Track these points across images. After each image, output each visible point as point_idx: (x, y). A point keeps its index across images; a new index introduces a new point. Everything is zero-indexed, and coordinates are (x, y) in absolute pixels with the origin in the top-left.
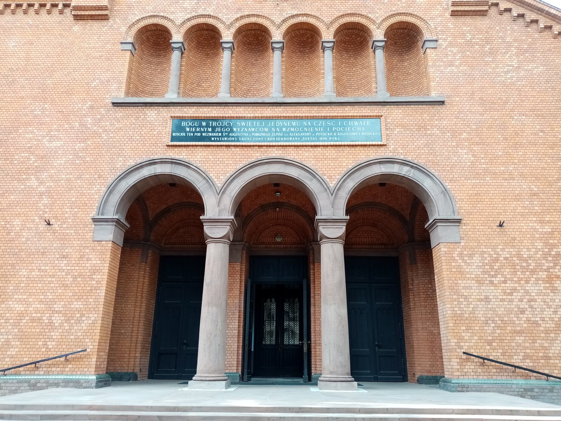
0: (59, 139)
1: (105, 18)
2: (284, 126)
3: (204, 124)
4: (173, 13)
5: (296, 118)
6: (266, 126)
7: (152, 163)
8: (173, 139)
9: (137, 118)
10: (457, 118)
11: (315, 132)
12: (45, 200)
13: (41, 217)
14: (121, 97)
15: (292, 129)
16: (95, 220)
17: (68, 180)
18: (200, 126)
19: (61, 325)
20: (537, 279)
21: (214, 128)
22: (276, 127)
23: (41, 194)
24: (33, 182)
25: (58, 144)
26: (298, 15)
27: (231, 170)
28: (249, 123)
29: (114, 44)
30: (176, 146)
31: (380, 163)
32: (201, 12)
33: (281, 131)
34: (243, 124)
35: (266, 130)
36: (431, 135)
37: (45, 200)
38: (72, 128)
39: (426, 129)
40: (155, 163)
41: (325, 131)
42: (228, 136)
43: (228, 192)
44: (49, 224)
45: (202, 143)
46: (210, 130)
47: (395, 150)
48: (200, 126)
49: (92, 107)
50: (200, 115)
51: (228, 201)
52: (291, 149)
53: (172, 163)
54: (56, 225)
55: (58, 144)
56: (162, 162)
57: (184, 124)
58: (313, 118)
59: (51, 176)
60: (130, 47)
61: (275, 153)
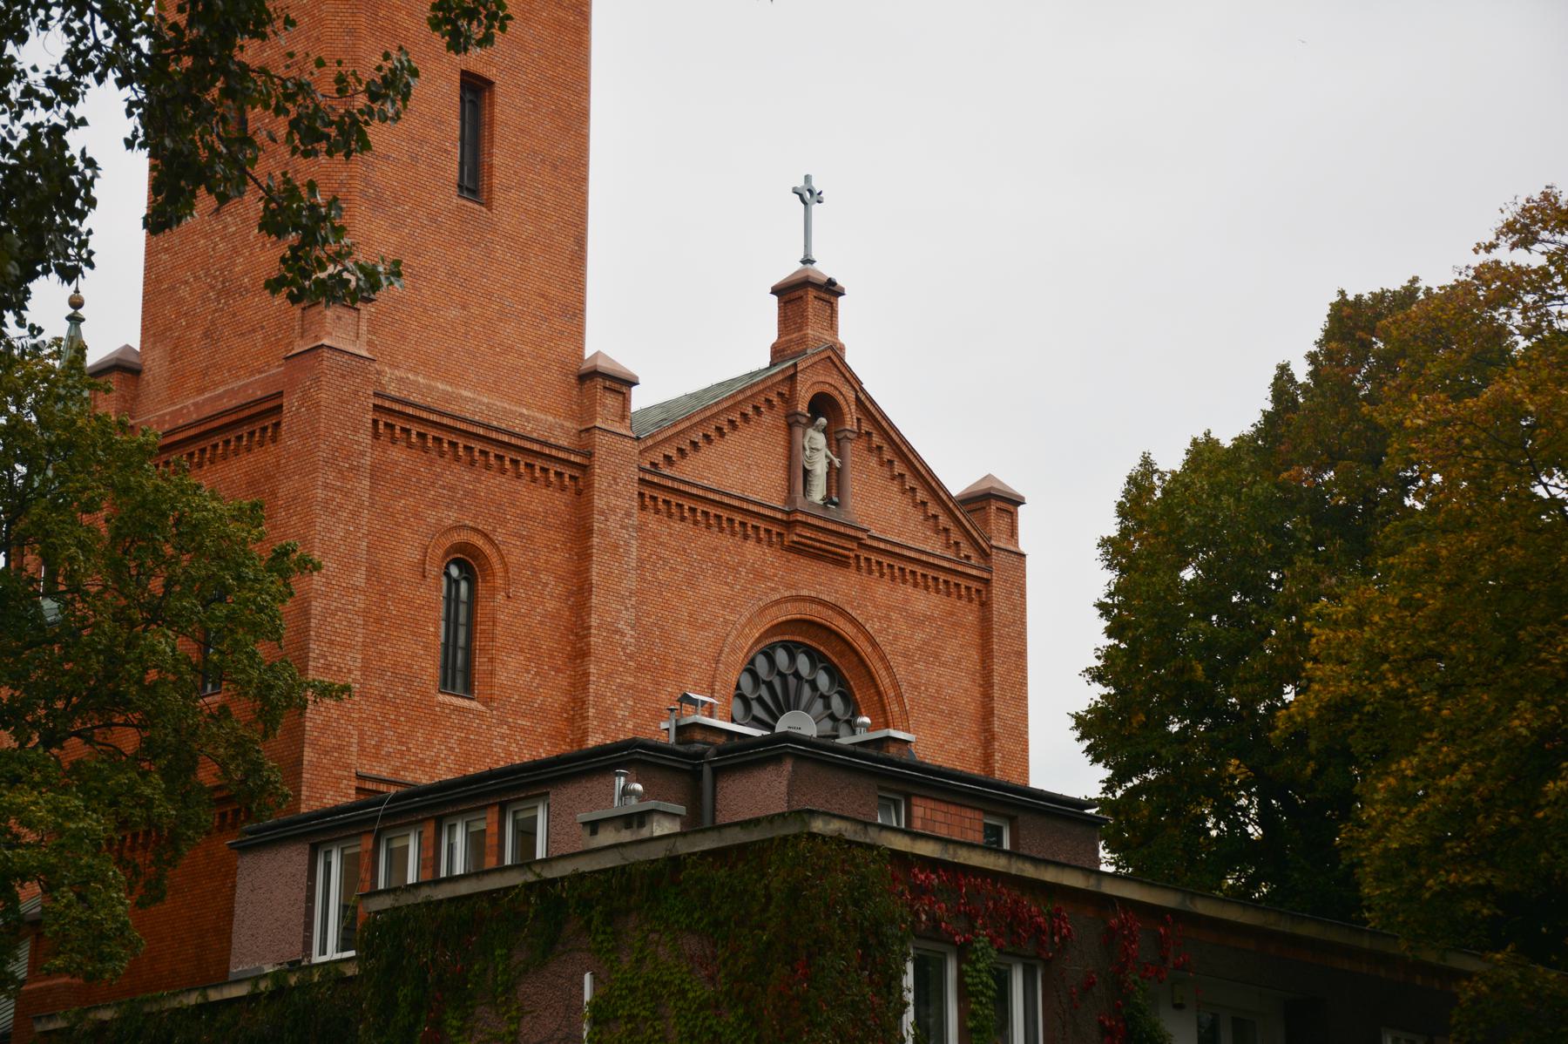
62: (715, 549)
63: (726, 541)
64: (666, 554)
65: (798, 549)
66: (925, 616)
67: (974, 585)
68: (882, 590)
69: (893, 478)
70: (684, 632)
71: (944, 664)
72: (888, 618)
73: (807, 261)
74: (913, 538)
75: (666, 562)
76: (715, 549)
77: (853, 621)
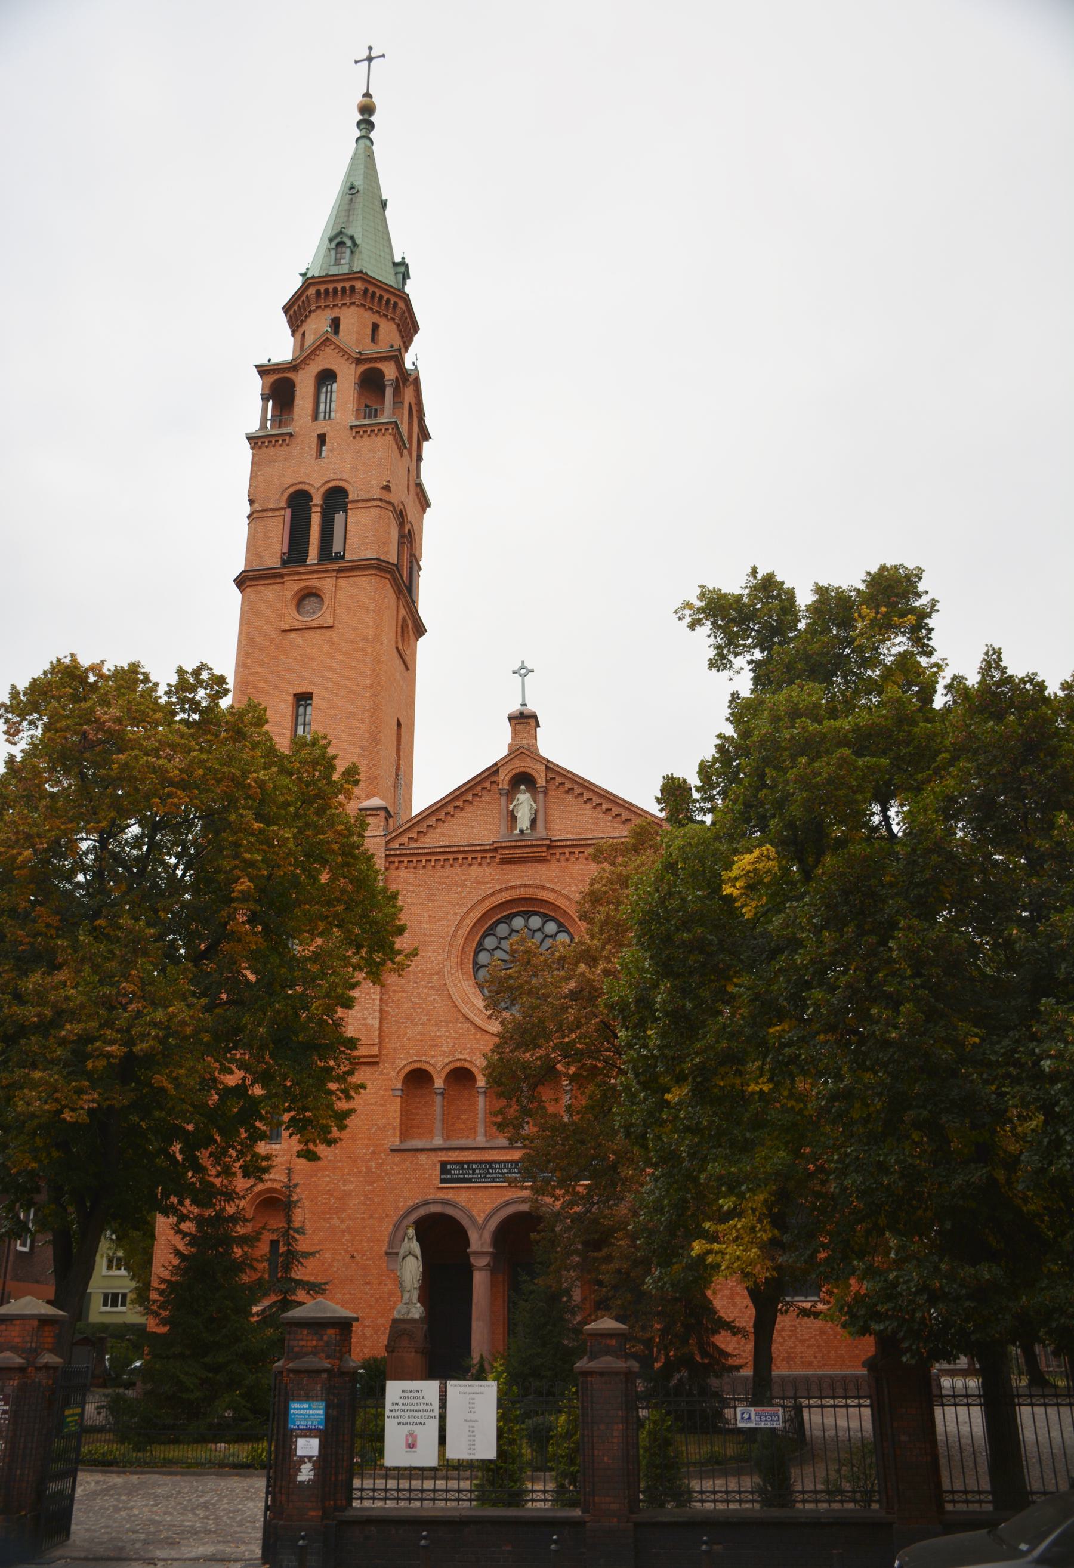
0: (352, 1183)
1: (377, 1063)
4: (433, 1057)
7: (426, 1203)
9: (411, 1162)
12: (347, 1237)
13: (346, 1251)
14: (396, 1142)
16: (387, 1254)
17: (363, 1218)
18: (463, 1168)
19: (371, 1336)
20: (723, 1296)
21: (474, 1170)
23: (343, 1231)
24: (335, 1221)
25: (352, 1186)
27: (489, 1208)
28: (502, 1166)
29: (386, 1090)
37: (347, 1237)
38: (360, 1172)
44: (353, 1256)
48: (463, 1168)
49: (374, 1152)
51: (487, 1235)
54: (358, 1258)
55: (352, 1186)
57: (449, 1167)
59: (349, 1216)
60: (399, 1093)
62: (448, 877)
63: (457, 870)
64: (410, 888)
65: (504, 861)
69: (585, 802)
70: (425, 926)
73: (524, 705)
74: (603, 832)
75: (412, 892)
76: (448, 877)
77: (552, 890)
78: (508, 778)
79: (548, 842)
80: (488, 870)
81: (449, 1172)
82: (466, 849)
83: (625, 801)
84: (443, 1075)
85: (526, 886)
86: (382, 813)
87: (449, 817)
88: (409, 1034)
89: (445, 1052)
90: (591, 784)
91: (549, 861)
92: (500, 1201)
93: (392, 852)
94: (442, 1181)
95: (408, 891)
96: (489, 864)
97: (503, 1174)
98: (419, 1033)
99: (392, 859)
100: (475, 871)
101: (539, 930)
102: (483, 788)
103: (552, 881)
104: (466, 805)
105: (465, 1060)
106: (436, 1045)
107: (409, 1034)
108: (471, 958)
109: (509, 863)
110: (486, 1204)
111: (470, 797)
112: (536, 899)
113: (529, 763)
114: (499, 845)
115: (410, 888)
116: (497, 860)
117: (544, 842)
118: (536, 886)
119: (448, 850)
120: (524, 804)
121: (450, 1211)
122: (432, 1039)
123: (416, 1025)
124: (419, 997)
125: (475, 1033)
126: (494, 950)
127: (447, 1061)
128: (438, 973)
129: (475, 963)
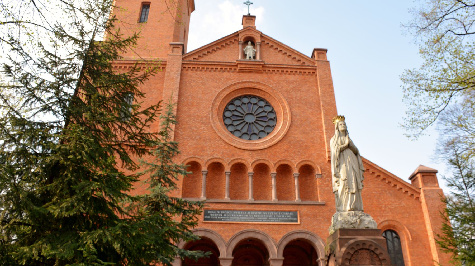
2: (255, 214)
3: (219, 212)
4: (202, 156)
5: (260, 211)
6: (246, 214)
8: (205, 219)
10: (330, 212)
11: (268, 217)
15: (259, 216)
18: (217, 213)
21: (223, 214)
22: (251, 215)
26: (260, 160)
27: (231, 235)
28: (239, 213)
30: (206, 223)
31: (297, 233)
32: (215, 156)
33: (254, 216)
34: (236, 213)
35: (247, 216)
36: (319, 220)
39: (317, 217)
40: (197, 231)
41: (273, 217)
42: (229, 219)
43: (231, 245)
45: (218, 222)
46: (221, 215)
47: (303, 227)
50: (217, 208)
51: (231, 251)
52: (258, 226)
53: (205, 231)
56: (200, 231)
57: (209, 212)
58: (268, 211)
61: (251, 228)
62: (212, 76)
63: (217, 73)
64: (193, 79)
65: (241, 71)
66: (294, 81)
67: (311, 71)
68: (276, 77)
71: (303, 91)
72: (279, 83)
75: (194, 81)
76: (212, 76)
77: (264, 85)
78: (243, 38)
79: (263, 63)
80: (232, 74)
81: (209, 215)
82: (222, 64)
83: (298, 52)
84: (207, 165)
85: (251, 82)
86: (181, 47)
87: (214, 51)
88: (190, 144)
89: (208, 154)
90: (282, 44)
91: (262, 73)
92: (237, 232)
93: (185, 62)
94: (205, 219)
95: (192, 80)
96: (233, 72)
97: (240, 217)
98: (195, 144)
99: (185, 66)
100: (226, 74)
101: (256, 104)
102: (231, 42)
103: (264, 81)
104: (222, 48)
105: (219, 158)
106: (204, 150)
107: (190, 144)
108: (222, 113)
109: (243, 72)
110: (230, 232)
111: (224, 44)
112: (256, 89)
113: (253, 33)
114: (239, 62)
115: (193, 79)
116: (237, 70)
117: (261, 63)
118: (257, 83)
119: (213, 63)
120: (250, 50)
121: (209, 236)
122: (202, 147)
123: (193, 140)
124: (196, 127)
125: (225, 146)
126: (233, 111)
127: (209, 158)
128: (206, 117)
129: (224, 116)
